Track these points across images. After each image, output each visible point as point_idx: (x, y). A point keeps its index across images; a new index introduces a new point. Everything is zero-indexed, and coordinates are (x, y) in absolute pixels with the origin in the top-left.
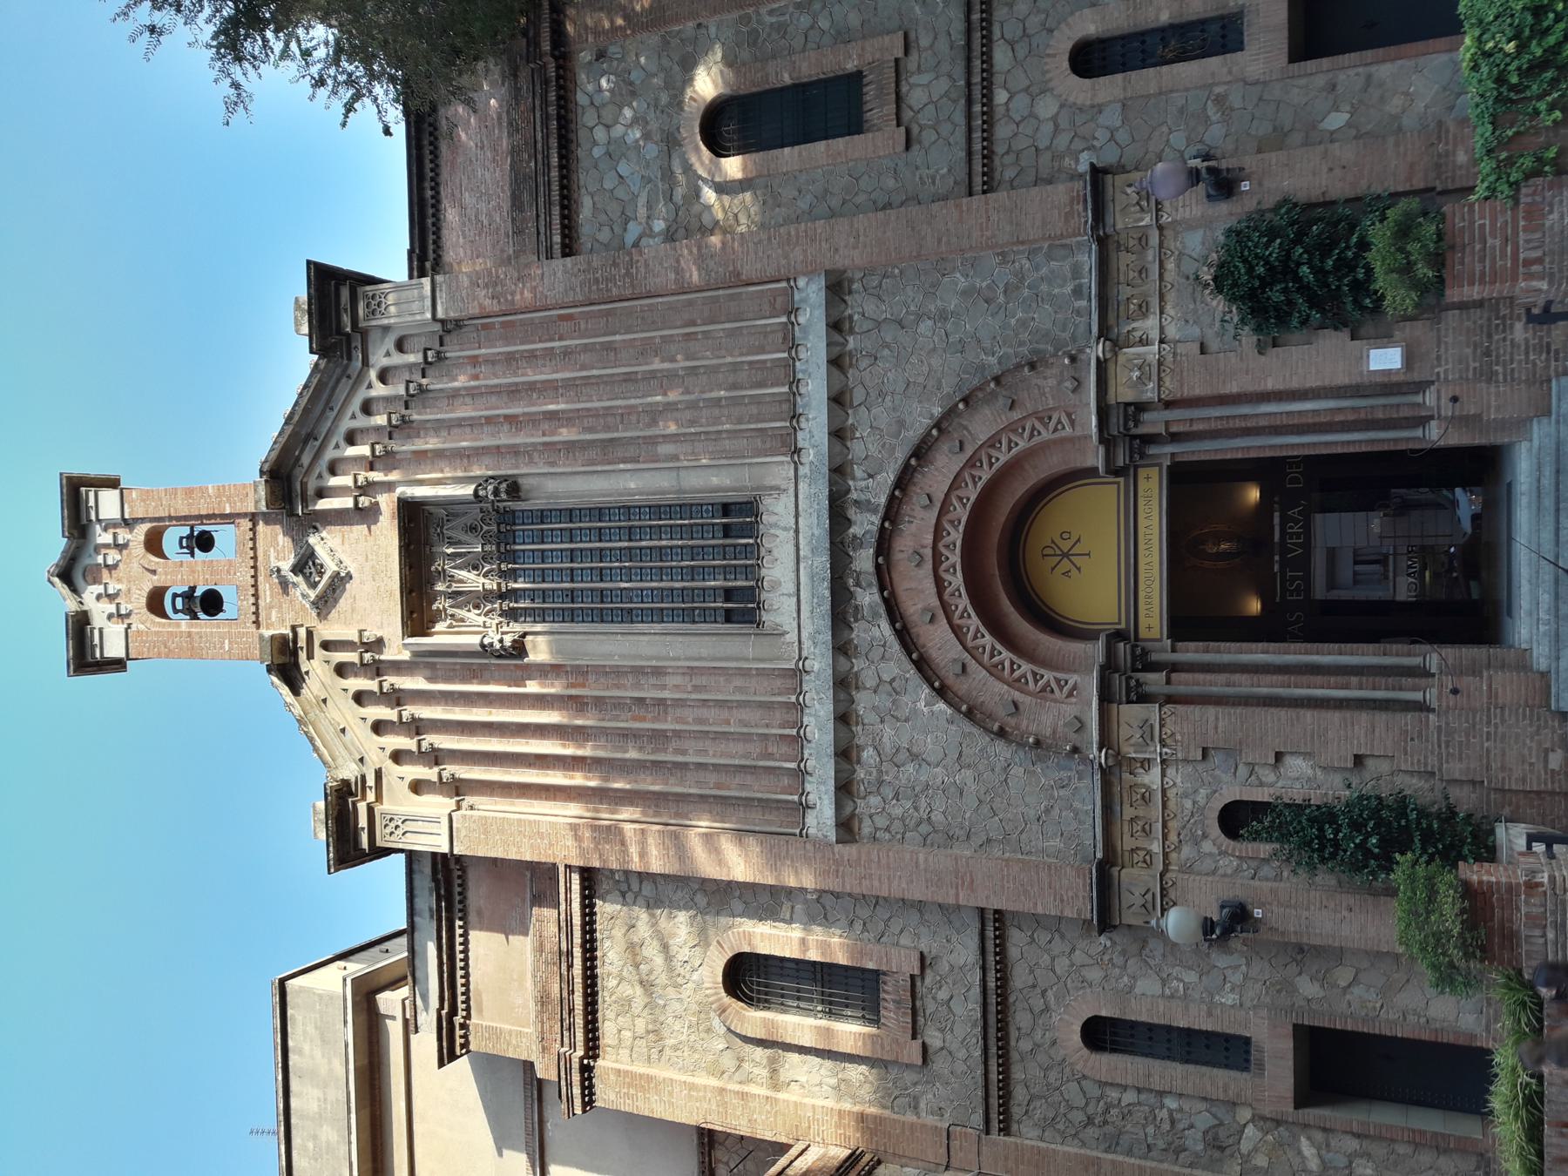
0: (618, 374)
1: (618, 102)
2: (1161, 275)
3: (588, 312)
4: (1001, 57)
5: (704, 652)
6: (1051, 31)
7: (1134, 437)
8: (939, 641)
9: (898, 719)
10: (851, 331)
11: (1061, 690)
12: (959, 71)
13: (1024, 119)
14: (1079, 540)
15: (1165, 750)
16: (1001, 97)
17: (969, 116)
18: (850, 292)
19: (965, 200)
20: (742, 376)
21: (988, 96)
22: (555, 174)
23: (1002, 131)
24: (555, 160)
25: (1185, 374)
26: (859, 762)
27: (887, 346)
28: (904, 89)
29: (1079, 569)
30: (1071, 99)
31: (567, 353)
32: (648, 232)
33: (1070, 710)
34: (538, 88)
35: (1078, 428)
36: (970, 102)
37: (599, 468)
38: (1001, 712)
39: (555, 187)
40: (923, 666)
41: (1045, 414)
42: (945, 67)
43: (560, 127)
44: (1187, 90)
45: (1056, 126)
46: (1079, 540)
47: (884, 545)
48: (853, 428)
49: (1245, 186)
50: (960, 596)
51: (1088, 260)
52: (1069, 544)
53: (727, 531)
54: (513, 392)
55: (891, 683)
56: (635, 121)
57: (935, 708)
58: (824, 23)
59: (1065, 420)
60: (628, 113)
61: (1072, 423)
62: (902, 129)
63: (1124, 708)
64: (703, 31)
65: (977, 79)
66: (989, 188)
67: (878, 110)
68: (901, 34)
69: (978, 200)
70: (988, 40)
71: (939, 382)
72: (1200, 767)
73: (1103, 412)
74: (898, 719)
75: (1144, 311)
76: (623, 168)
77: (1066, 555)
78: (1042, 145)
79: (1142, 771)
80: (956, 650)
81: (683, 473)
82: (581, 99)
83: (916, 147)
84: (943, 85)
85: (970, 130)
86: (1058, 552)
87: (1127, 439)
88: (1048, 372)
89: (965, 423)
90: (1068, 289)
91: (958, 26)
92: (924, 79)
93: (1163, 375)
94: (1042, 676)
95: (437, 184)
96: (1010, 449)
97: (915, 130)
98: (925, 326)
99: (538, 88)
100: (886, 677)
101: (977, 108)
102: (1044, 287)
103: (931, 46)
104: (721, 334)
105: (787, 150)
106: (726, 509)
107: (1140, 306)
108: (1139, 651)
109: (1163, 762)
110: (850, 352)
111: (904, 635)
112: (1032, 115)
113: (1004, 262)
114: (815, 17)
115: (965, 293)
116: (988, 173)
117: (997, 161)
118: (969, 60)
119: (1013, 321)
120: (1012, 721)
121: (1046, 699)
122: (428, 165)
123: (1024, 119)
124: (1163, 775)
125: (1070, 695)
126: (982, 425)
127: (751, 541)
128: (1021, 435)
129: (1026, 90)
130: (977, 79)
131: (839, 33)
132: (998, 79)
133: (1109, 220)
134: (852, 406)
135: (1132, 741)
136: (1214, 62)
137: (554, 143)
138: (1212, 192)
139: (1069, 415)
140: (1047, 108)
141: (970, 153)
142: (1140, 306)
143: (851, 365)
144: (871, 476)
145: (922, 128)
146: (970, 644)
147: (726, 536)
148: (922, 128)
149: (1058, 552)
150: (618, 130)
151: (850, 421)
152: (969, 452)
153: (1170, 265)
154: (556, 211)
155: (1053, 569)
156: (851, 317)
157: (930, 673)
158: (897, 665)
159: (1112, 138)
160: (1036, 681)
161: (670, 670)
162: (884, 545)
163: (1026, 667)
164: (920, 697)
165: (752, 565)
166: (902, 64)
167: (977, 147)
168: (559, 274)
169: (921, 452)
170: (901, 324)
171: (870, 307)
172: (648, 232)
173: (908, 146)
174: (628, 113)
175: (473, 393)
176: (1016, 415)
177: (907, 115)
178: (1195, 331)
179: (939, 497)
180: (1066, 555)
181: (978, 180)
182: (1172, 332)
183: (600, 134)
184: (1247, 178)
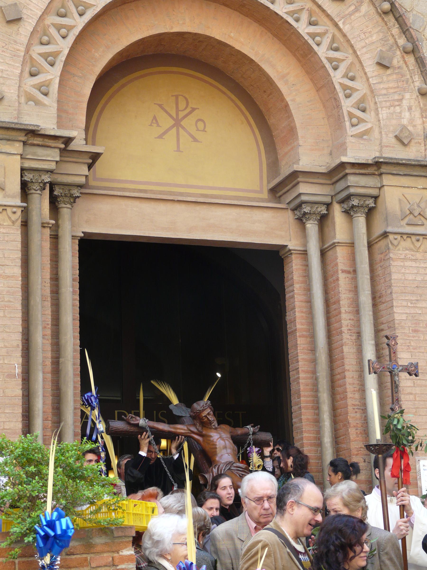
7: (328, 205)
11: (34, 86)
14: (195, 140)
25: (414, 264)
29: (161, 137)
35: (353, 140)
41: (370, 105)
46: (195, 140)
52: (192, 130)
59: (362, 128)
61: (360, 136)
77: (177, 123)
86: (181, 114)
87: (328, 200)
88: (417, 114)
93: (414, 238)
94: (52, 65)
96: (330, 60)
121: (24, 63)
125: (30, 98)
128: (346, 76)
139: (366, 132)
149: (181, 116)
155: (160, 106)
160: (45, 56)
180: (177, 123)
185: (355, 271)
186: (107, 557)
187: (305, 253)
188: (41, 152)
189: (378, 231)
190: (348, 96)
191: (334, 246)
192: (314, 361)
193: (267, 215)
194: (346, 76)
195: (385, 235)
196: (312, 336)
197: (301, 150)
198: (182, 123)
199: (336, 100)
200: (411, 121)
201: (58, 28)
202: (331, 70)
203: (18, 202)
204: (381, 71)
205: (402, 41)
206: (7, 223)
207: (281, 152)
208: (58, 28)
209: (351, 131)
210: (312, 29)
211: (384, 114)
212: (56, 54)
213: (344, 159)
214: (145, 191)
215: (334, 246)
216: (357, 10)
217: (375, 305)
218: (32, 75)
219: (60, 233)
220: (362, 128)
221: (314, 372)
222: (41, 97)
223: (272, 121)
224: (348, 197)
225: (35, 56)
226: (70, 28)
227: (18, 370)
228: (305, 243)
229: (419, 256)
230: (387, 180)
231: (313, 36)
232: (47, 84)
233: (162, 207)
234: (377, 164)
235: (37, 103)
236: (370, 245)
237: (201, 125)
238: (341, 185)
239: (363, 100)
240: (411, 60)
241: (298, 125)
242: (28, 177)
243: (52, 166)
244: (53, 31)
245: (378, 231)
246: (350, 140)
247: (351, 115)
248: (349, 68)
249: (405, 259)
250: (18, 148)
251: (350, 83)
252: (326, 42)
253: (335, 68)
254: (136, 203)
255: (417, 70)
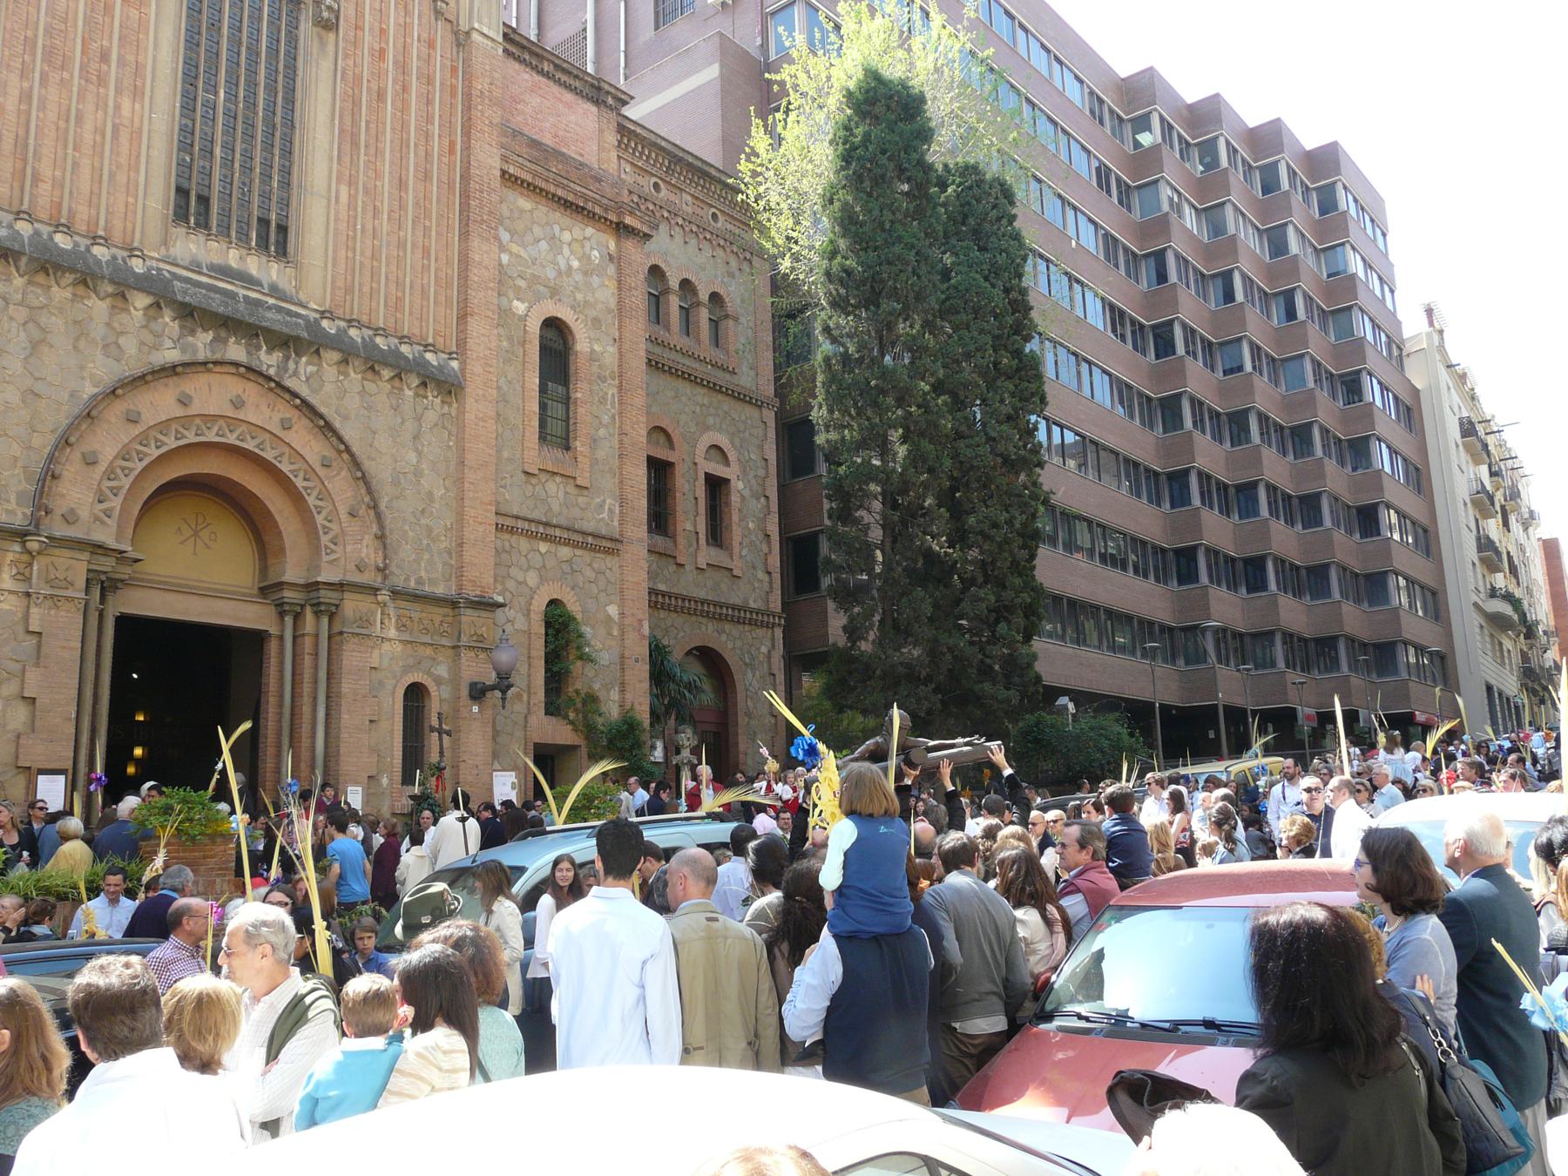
0: (408, 176)
1: (585, 258)
2: (424, 644)
3: (455, 170)
4: (565, 552)
5: (155, 153)
6: (573, 589)
7: (302, 606)
8: (159, 403)
9: (77, 339)
10: (417, 395)
12: (563, 521)
13: (528, 561)
14: (208, 547)
15: (41, 597)
16: (543, 547)
17: (539, 522)
18: (442, 402)
19: (493, 508)
20: (393, 287)
21: (546, 538)
22: (552, 189)
23: (524, 544)
24: (560, 192)
26: (30, 282)
27: (403, 423)
28: (558, 479)
30: (536, 597)
31: (428, 136)
32: (502, 248)
33: (84, 514)
34: (606, 201)
36: (546, 524)
37: (337, 122)
38: (86, 447)
39: (543, 185)
40: (140, 380)
42: (565, 511)
43: (577, 206)
44: (529, 676)
45: (520, 583)
46: (208, 547)
47: (252, 372)
48: (346, 375)
49: (475, 709)
50: (197, 435)
51: (440, 590)
53: (264, 222)
54: (403, 68)
55: (116, 343)
56: (570, 268)
57: (88, 383)
58: (602, 432)
59: (333, 557)
60: (575, 264)
61: (331, 562)
62: (537, 472)
63: (83, 567)
64: (612, 342)
65: (558, 533)
66: (499, 528)
67: (553, 457)
68: (588, 485)
69: (493, 519)
70: (576, 545)
71: (373, 459)
72: (20, 629)
73: (340, 586)
74: (77, 339)
75: (401, 627)
76: (543, 245)
77: (196, 534)
78: (514, 571)
79: (14, 571)
80: (149, 419)
81: (324, 202)
82: (590, 231)
83: (523, 476)
84: (556, 508)
85: (530, 521)
88: (372, 551)
89: (344, 473)
90: (423, 574)
91: (589, 526)
92: (561, 495)
95: (549, 78)
96: (316, 507)
97: (534, 481)
98: (412, 457)
99: (606, 201)
100: (122, 341)
101: (541, 530)
102: (426, 556)
103: (577, 504)
104: (425, 281)
105: (537, 381)
106: (283, 229)
107: (404, 626)
108: (119, 585)
109: (28, 595)
110: (402, 390)
111: (172, 370)
112: (529, 567)
113: (447, 530)
114: (606, 427)
115: (430, 494)
116: (512, 530)
117: (507, 536)
118: (568, 529)
119: (407, 528)
120: (75, 455)
122: (564, 78)
123: (528, 561)
124: (10, 592)
125: (97, 519)
126: (341, 486)
127: (253, 244)
128: (326, 519)
129: (544, 566)
130: (558, 533)
131: (595, 441)
132: (553, 548)
133: (469, 612)
134: (364, 379)
135: (51, 568)
136: (540, 695)
137: (571, 198)
138: (479, 686)
139: (334, 560)
140: (532, 579)
141: (517, 517)
142: (404, 626)
143: (393, 387)
144: (308, 379)
145: (534, 486)
146: (153, 433)
147: (259, 219)
148: (534, 486)
150: (566, 251)
151: (352, 374)
152: (321, 472)
153: (429, 651)
154: (529, 178)
155: (185, 520)
156: (426, 397)
157: (130, 388)
158: (134, 358)
159: (509, 621)
160: (111, 489)
161: (137, 106)
162: (252, 372)
163: (126, 483)
164: (103, 370)
165: (229, 236)
166: (572, 481)
167: (520, 524)
168: (490, 161)
169: (328, 429)
170: (416, 437)
171: (431, 416)
172: (502, 248)
173: (526, 473)
174: (575, 264)
175: (405, 28)
176: (344, 517)
177: (543, 477)
178: (386, 663)
179: (288, 436)
180: (196, 534)
181: (509, 522)
182: (386, 646)
183: (567, 236)
184: (480, 711)
185: (317, 654)
186: (222, 848)
187: (281, 638)
188: (102, 559)
189: (336, 629)
190: (325, 533)
191: (303, 635)
192: (280, 714)
193: (257, 607)
194: (326, 519)
195: (341, 633)
196: (281, 696)
197: (288, 566)
198: (200, 534)
199: (317, 534)
200: (368, 555)
201: (123, 469)
202: (316, 515)
203: (83, 595)
204: (350, 518)
205: (367, 499)
206: (74, 609)
207: (271, 561)
208: (123, 469)
209: (325, 558)
210: (306, 484)
211: (349, 548)
212: (119, 488)
213: (319, 579)
214: (166, 583)
215: (303, 635)
216: (338, 474)
217: (328, 679)
218: (100, 502)
219: (105, 613)
220: (333, 557)
221: (280, 721)
222: (106, 519)
223: (266, 538)
224: (319, 604)
225: (104, 488)
226: (131, 470)
227: (74, 716)
228: (283, 630)
229: (362, 649)
230: (347, 595)
231: (306, 488)
232: (112, 509)
233: (180, 597)
234: (342, 585)
235: (103, 523)
236: (330, 637)
237: (213, 536)
238: (314, 595)
239: (336, 537)
240: (372, 513)
241: (287, 546)
242: (91, 575)
243: (109, 569)
244: (118, 471)
245: (336, 629)
246: (323, 565)
247: (326, 547)
248: (329, 514)
249: (353, 651)
250: (86, 556)
251: (328, 524)
252: (315, 493)
253: (319, 513)
254: (161, 592)
255: (375, 520)
